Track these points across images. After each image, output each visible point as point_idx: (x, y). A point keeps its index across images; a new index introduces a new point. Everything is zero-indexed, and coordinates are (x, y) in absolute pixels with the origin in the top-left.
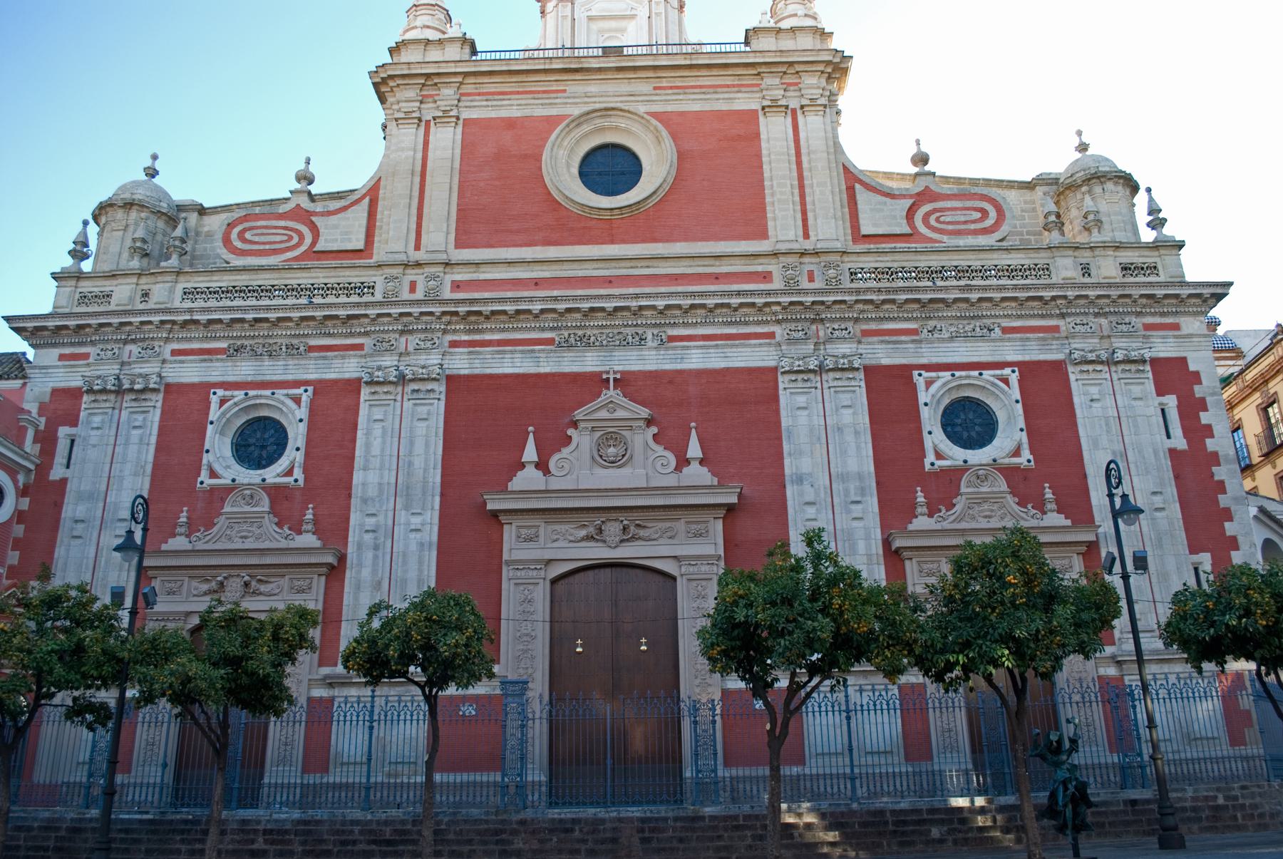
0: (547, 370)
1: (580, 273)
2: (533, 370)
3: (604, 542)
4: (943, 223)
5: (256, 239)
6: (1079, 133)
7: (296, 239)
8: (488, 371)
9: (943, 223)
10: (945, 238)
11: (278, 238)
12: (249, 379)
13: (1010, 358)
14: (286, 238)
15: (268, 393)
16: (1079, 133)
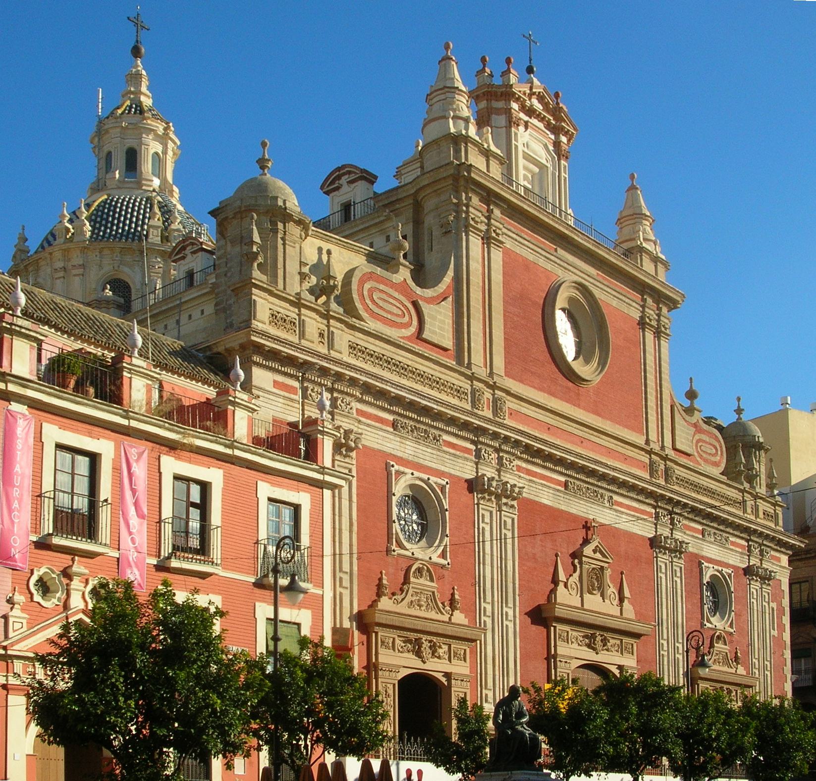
0: (563, 508)
1: (570, 429)
2: (556, 506)
3: (594, 649)
4: (702, 451)
5: (381, 303)
6: (739, 399)
7: (407, 319)
8: (537, 499)
9: (702, 451)
10: (702, 463)
11: (396, 311)
12: (411, 458)
13: (731, 562)
14: (400, 312)
15: (425, 477)
16: (739, 399)
